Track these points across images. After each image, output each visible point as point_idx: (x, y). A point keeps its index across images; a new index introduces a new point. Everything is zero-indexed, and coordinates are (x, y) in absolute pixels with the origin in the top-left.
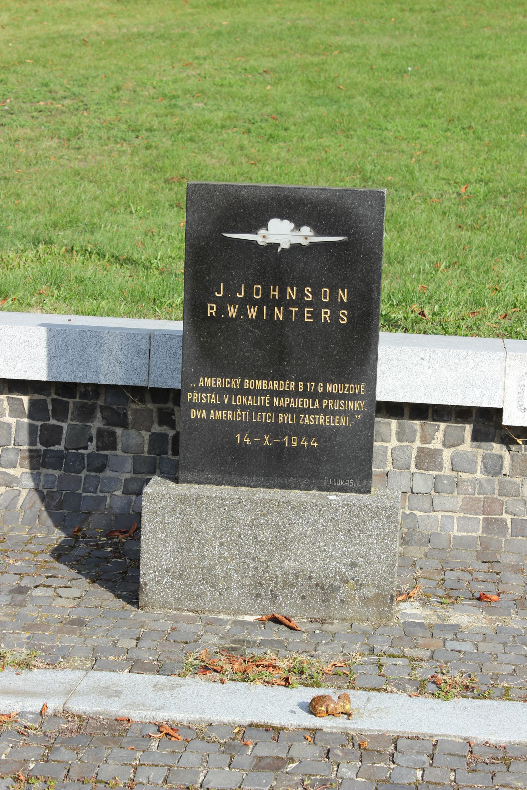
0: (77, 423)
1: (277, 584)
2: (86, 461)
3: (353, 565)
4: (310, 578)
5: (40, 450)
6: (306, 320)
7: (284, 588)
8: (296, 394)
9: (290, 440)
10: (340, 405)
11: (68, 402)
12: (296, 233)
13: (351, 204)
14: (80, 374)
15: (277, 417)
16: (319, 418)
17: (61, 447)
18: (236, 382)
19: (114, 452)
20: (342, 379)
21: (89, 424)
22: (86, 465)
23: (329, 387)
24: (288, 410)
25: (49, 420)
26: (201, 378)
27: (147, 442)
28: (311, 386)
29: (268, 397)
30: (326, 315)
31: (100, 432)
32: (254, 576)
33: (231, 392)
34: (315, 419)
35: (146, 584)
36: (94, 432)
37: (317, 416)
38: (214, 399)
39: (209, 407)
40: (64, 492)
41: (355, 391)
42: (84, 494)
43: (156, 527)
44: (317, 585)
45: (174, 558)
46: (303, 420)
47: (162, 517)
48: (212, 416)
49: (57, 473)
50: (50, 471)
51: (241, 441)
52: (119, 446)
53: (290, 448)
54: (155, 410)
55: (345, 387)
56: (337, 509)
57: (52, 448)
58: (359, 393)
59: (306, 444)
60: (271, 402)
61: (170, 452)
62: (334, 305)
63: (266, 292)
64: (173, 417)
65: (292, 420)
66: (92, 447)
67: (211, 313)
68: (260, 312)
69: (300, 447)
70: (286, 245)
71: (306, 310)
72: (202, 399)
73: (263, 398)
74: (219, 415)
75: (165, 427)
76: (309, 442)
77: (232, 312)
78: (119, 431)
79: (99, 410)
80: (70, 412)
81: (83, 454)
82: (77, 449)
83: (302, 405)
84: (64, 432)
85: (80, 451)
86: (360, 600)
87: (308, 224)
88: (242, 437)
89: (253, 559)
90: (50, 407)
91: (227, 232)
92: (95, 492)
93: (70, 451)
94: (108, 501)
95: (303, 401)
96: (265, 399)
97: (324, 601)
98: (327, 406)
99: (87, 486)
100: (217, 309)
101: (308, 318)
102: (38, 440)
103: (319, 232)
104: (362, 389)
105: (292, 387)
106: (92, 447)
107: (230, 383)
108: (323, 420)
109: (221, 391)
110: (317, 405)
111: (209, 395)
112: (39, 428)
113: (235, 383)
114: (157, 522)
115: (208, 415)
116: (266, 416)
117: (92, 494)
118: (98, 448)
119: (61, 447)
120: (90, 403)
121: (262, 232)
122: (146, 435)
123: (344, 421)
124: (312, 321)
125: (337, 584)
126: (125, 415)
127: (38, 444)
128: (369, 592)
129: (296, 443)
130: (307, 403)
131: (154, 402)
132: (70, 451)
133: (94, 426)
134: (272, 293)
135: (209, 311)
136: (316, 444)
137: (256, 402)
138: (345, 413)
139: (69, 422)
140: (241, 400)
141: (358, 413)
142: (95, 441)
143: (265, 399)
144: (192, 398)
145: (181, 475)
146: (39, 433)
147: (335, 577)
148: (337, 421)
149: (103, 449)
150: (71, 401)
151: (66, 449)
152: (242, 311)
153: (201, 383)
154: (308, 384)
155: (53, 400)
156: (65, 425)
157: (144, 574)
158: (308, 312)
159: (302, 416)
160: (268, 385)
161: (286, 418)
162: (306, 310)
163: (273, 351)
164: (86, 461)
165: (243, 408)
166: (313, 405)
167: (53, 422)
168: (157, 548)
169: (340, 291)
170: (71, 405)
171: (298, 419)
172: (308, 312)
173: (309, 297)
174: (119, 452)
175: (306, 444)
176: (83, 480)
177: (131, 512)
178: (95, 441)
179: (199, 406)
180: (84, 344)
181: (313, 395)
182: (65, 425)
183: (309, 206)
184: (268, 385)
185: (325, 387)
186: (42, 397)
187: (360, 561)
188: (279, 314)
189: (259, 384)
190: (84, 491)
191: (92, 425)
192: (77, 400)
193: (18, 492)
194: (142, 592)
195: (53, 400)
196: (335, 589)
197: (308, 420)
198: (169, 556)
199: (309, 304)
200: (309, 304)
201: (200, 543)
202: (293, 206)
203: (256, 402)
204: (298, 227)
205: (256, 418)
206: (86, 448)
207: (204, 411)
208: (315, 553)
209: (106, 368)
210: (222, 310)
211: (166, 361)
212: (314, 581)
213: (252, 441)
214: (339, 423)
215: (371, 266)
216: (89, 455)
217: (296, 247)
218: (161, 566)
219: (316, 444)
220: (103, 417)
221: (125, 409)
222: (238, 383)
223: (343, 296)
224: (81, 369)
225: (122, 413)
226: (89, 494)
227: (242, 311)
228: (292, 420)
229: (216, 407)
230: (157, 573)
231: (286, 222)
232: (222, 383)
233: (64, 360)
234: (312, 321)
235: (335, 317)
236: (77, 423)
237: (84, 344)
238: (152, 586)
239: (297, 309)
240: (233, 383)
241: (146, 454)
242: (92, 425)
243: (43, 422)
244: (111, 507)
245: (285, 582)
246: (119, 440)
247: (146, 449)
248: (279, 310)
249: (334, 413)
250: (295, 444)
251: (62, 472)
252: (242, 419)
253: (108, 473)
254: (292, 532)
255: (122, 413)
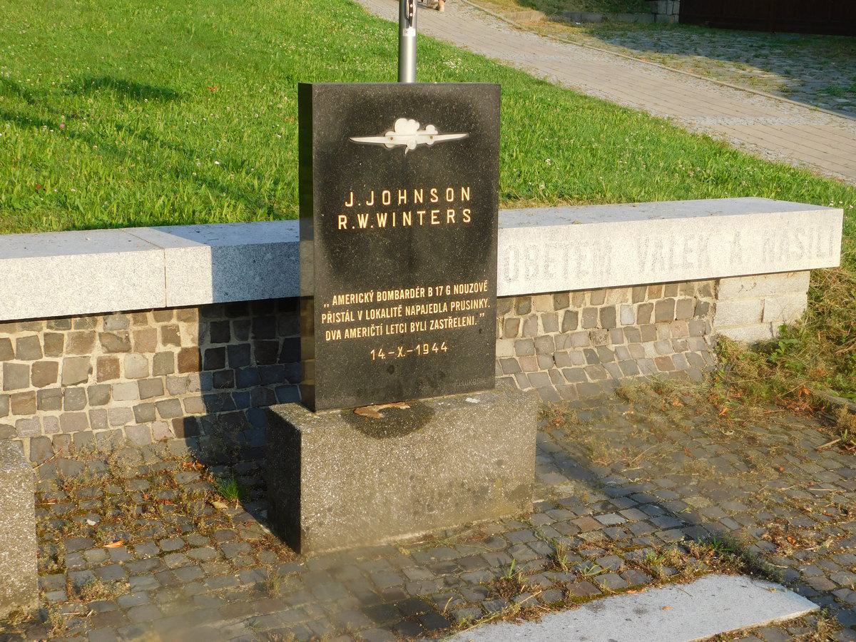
0: (74, 356)
1: (432, 498)
2: (87, 395)
3: (500, 463)
4: (463, 485)
5: (33, 391)
6: (433, 223)
7: (439, 501)
8: (425, 301)
9: (422, 348)
10: (466, 306)
11: (63, 335)
12: (422, 132)
13: (471, 99)
14: (91, 304)
15: (409, 327)
16: (448, 321)
17: (57, 385)
18: (369, 297)
19: (116, 381)
20: (467, 279)
21: (87, 355)
22: (88, 399)
23: (456, 289)
24: (420, 318)
25: (41, 357)
26: (335, 297)
27: (151, 363)
28: (439, 289)
29: (400, 307)
30: (451, 215)
31: (101, 363)
32: (412, 496)
33: (366, 307)
34: (444, 323)
35: (308, 529)
36: (93, 363)
37: (446, 320)
38: (348, 317)
39: (343, 327)
40: (72, 433)
41: (479, 290)
42: (95, 431)
43: (316, 467)
44: (469, 490)
45: (336, 496)
46: (434, 326)
47: (323, 455)
48: (347, 335)
49: (57, 413)
50: (49, 413)
51: (376, 357)
52: (122, 373)
53: (422, 356)
54: (159, 330)
55: (470, 287)
56: (486, 412)
57: (47, 387)
58: (483, 290)
59: (437, 349)
60: (403, 312)
61: (176, 370)
62: (458, 204)
63: (395, 199)
64: (178, 333)
65: (423, 327)
66: (92, 379)
67: (342, 226)
68: (389, 220)
69: (432, 353)
70: (412, 147)
71: (433, 212)
72: (336, 318)
73: (395, 308)
74: (353, 333)
75: (169, 346)
76: (439, 346)
77: (363, 222)
78: (121, 357)
79: (97, 337)
80: (65, 345)
81: (83, 389)
82: (76, 384)
83: (432, 310)
84: (60, 367)
85: (79, 386)
86: (506, 496)
87: (432, 123)
88: (377, 352)
89: (411, 478)
90: (42, 343)
91: (354, 136)
92: (106, 427)
93: (69, 387)
94: (124, 435)
95: (432, 307)
96: (397, 310)
97: (475, 504)
98: (454, 308)
99: (94, 422)
100: (348, 220)
101: (435, 220)
102: (31, 382)
103: (442, 130)
104: (485, 287)
105: (422, 293)
106: (92, 379)
107: (363, 298)
108: (451, 323)
109: (354, 308)
110: (445, 309)
111: (343, 313)
112: (31, 368)
113: (367, 297)
114: (318, 462)
115: (343, 334)
116: (398, 327)
117: (104, 430)
118: (99, 379)
119: (57, 385)
120: (86, 331)
121: (389, 133)
122: (150, 356)
123: (470, 321)
124: (439, 223)
125: (486, 484)
126: (127, 338)
127: (31, 385)
128: (512, 487)
129: (427, 350)
130: (436, 308)
131: (157, 321)
132: (69, 387)
133: (93, 355)
134: (400, 198)
135: (340, 223)
136: (446, 348)
137: (389, 314)
138: (470, 313)
139: (65, 355)
140: (375, 314)
141: (481, 310)
142: (95, 372)
143: (397, 310)
144: (326, 320)
145: (318, 403)
146: (31, 373)
147: (484, 478)
148: (464, 321)
149: (105, 378)
150: (65, 332)
151: (63, 385)
152: (373, 221)
153: (334, 302)
154: (437, 288)
155: (46, 335)
156: (60, 360)
157: (306, 518)
158: (435, 214)
159: (433, 321)
160: (399, 295)
161: (417, 326)
162: (433, 212)
163: (406, 259)
164: (87, 395)
165: (377, 322)
166: (442, 309)
167: (45, 359)
168: (317, 489)
169: (463, 189)
170: (66, 337)
171: (429, 325)
172: (435, 214)
173: (435, 199)
174: (122, 379)
175: (437, 349)
176: (88, 416)
177: (153, 441)
178: (95, 372)
179: (333, 327)
180: (92, 270)
181: (443, 299)
182: (60, 360)
183: (433, 103)
184: (399, 295)
185: (452, 289)
186: (33, 333)
187: (506, 458)
188: (407, 219)
189: (391, 295)
190: (94, 427)
191: (90, 355)
192: (73, 330)
193: (19, 443)
194: (305, 538)
195: (46, 335)
196: (484, 490)
197: (436, 325)
198: (330, 494)
199: (435, 206)
200: (435, 206)
201: (361, 474)
202: (417, 105)
203: (389, 314)
204: (423, 127)
205: (389, 331)
206: (86, 381)
207: (339, 331)
208: (467, 460)
209: (119, 293)
210: (353, 221)
211: (183, 277)
212: (466, 487)
213: (387, 355)
214: (465, 323)
215: (490, 161)
216: (90, 388)
217: (422, 148)
218: (323, 507)
219: (446, 348)
220: (103, 345)
221: (127, 333)
222: (371, 297)
223: (466, 194)
224: (91, 299)
225: (124, 337)
226: (100, 430)
227: (373, 221)
228: (423, 327)
229: (350, 325)
230: (319, 515)
231: (412, 122)
232: (355, 299)
233: (71, 291)
234: (439, 223)
235: (459, 217)
236: (74, 356)
237: (92, 270)
238: (315, 529)
239: (424, 212)
240: (366, 297)
241: (151, 377)
242: (90, 355)
243: (35, 361)
244: (129, 440)
245: (440, 494)
246: (122, 367)
247: (151, 372)
248: (407, 214)
249: (461, 314)
250: (427, 352)
251: (63, 411)
252: (376, 333)
253: (113, 404)
254: (447, 443)
255: (124, 337)
